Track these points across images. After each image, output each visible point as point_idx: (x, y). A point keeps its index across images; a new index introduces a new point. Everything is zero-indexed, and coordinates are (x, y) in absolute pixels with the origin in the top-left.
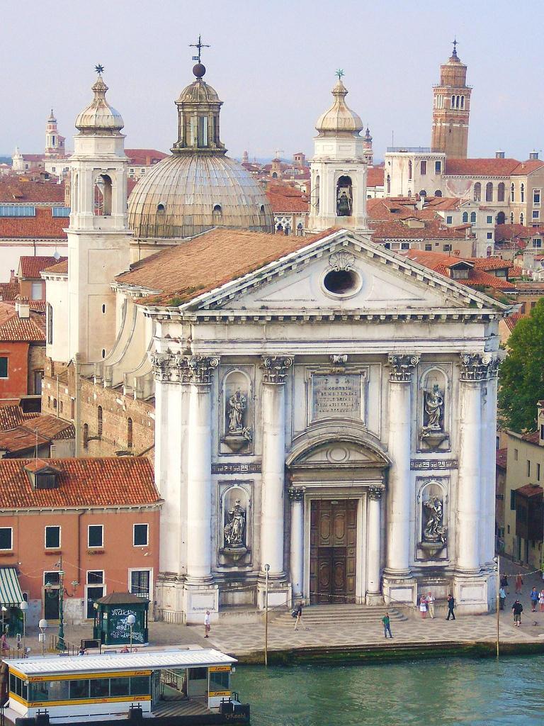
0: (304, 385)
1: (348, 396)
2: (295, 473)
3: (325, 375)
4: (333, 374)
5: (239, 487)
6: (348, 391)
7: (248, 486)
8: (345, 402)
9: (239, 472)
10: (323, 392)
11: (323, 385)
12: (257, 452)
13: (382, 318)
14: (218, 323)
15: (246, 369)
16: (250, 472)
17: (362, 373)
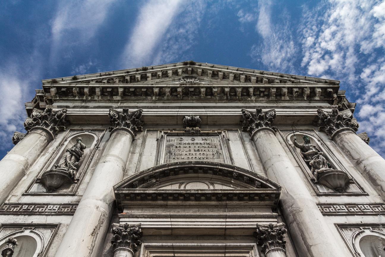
0: (155, 143)
1: (206, 149)
2: (129, 207)
3: (178, 135)
4: (188, 134)
5: (32, 235)
6: (206, 146)
7: (47, 234)
8: (205, 152)
9: (40, 214)
10: (178, 146)
11: (180, 142)
12: (80, 192)
13: (227, 90)
14: (77, 98)
15: (97, 133)
16: (59, 214)
17: (220, 133)
